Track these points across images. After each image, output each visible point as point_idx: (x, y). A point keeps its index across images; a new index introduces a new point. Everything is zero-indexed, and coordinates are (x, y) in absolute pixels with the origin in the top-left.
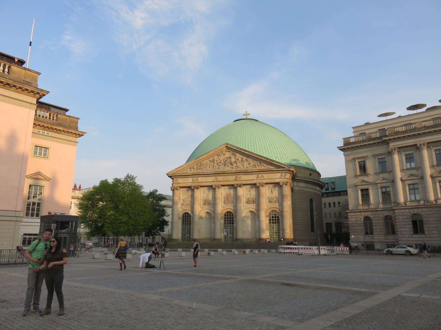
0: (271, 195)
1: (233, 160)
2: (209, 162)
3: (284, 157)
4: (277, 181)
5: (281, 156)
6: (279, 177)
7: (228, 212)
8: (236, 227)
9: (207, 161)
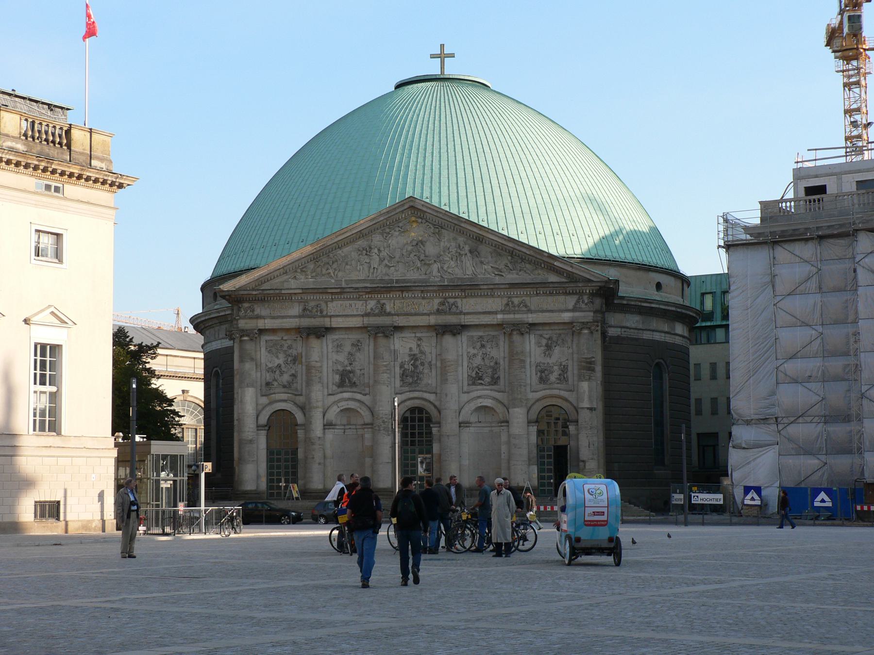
0: (548, 360)
1: (431, 249)
2: (354, 255)
3: (580, 232)
4: (567, 316)
5: (571, 228)
6: (571, 307)
7: (412, 410)
8: (440, 455)
9: (346, 250)
